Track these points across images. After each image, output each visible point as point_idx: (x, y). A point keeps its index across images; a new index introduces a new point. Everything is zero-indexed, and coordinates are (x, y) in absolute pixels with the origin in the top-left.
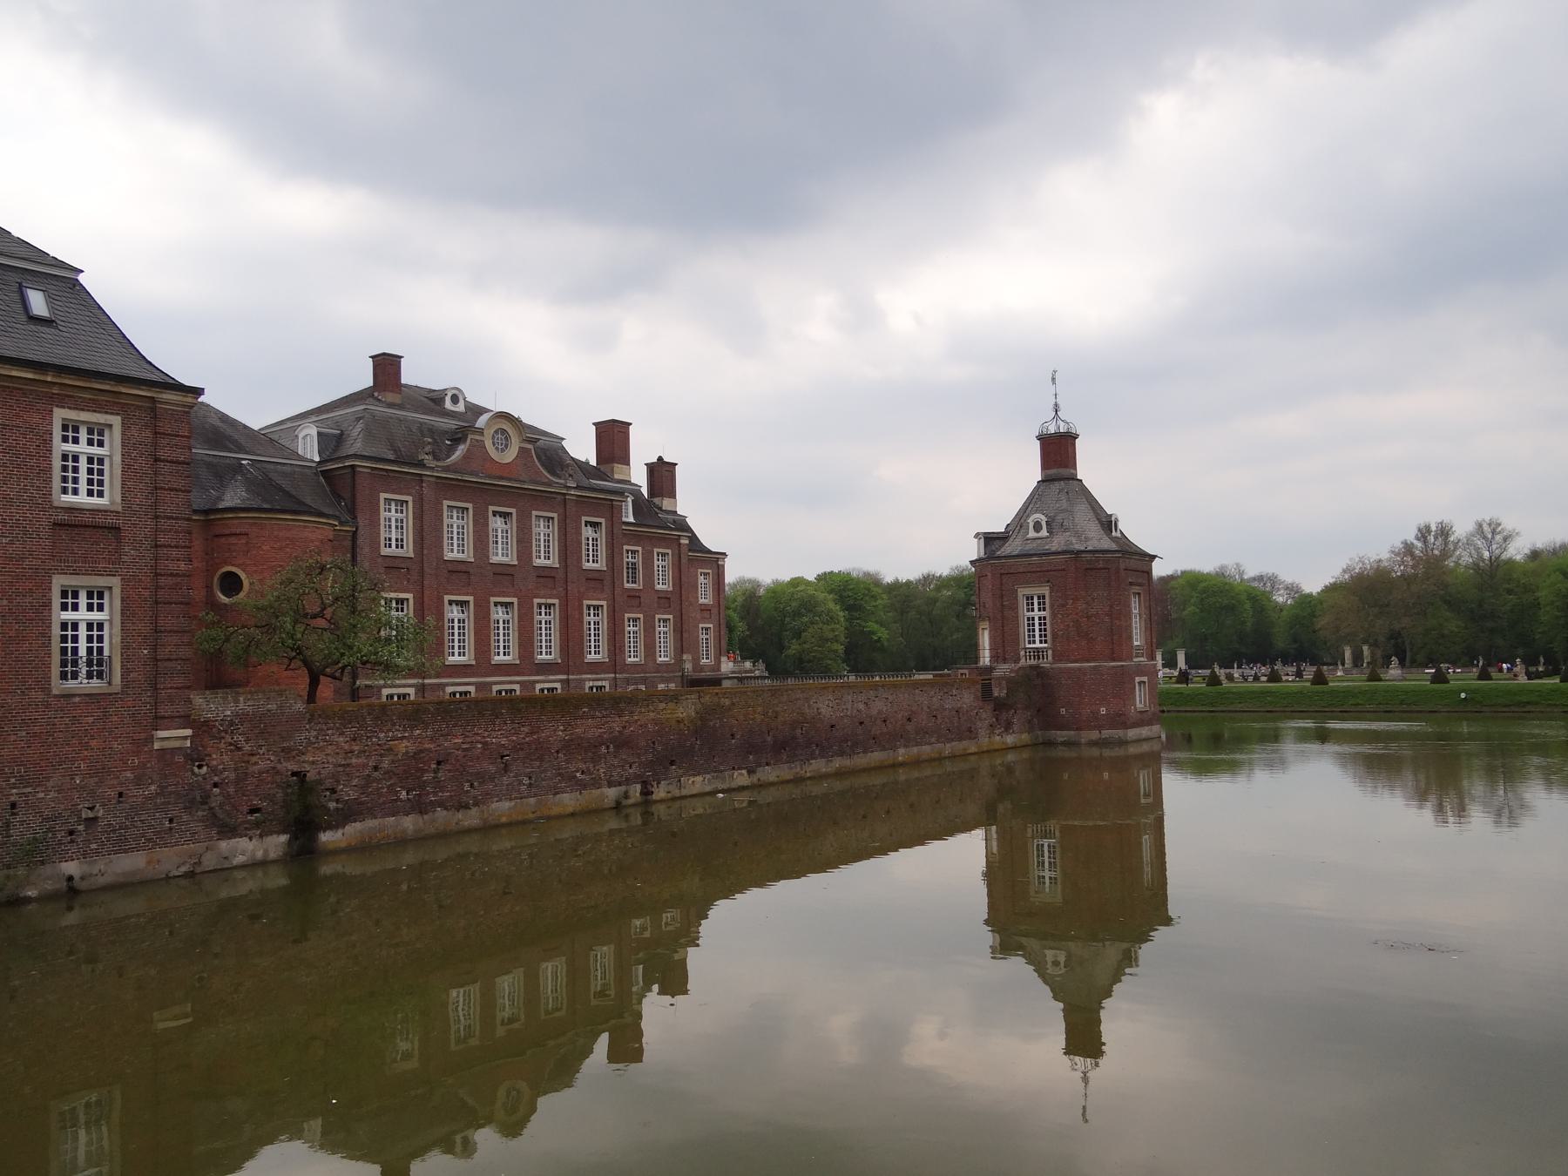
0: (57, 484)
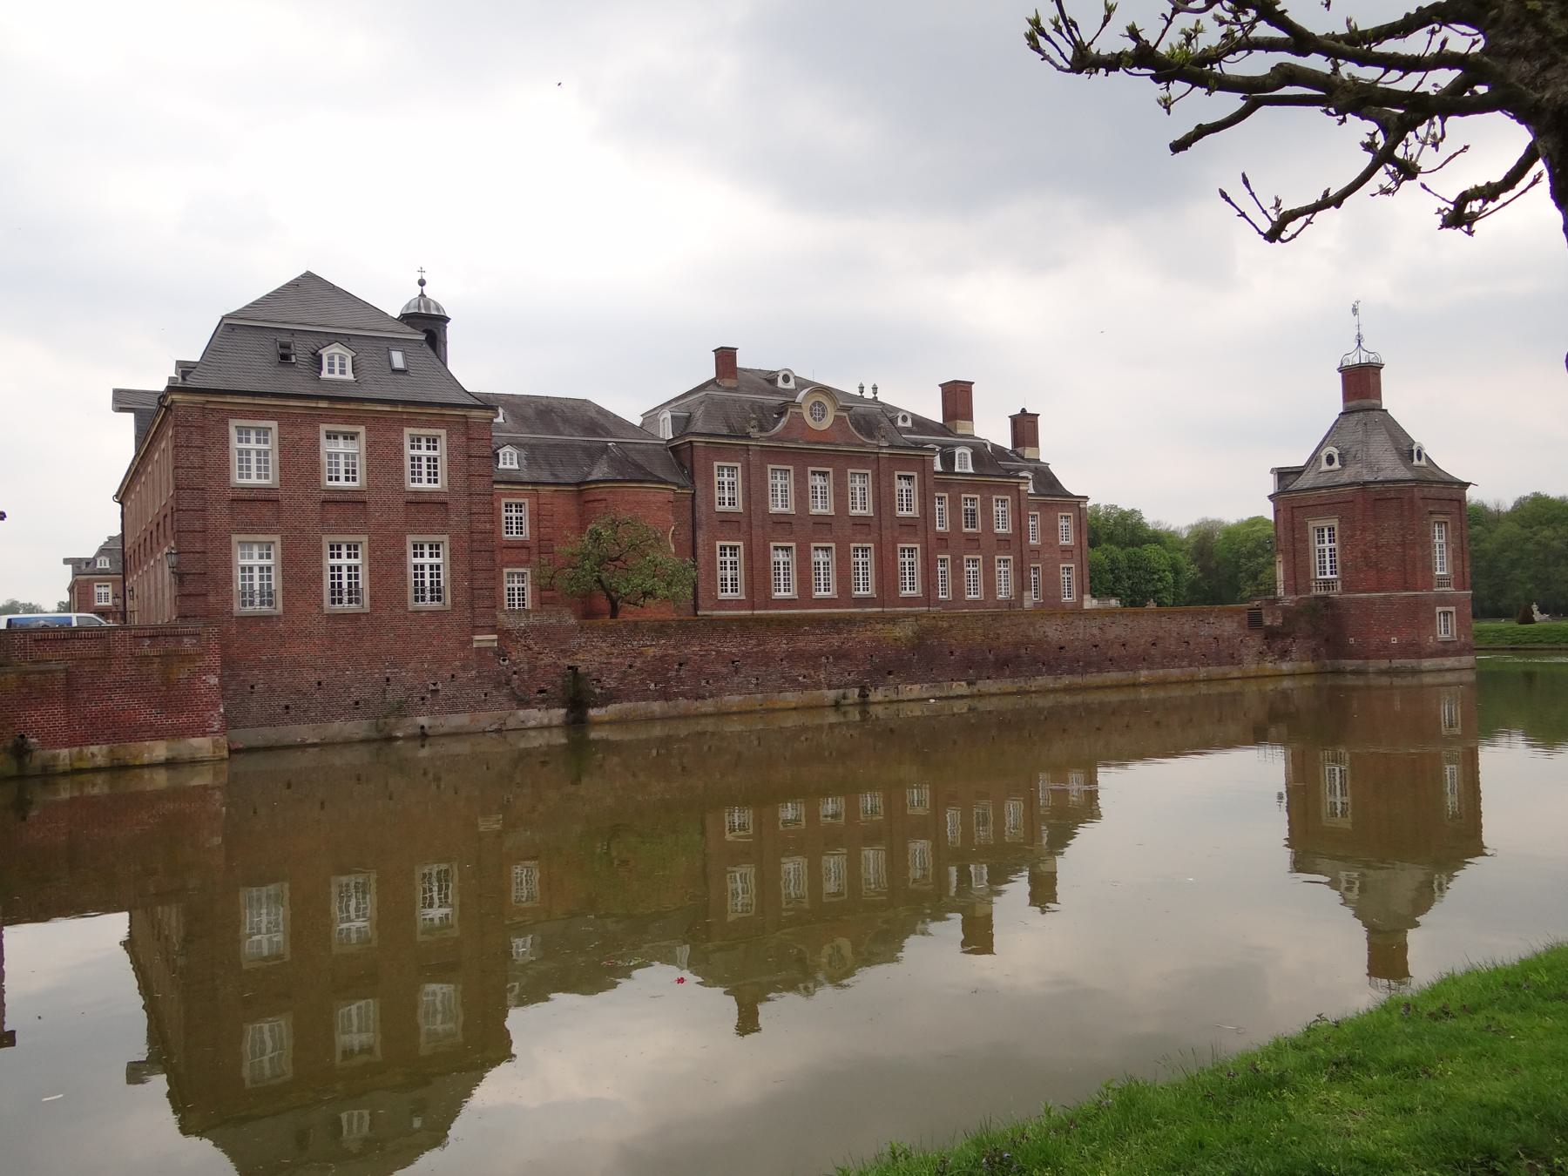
0: (408, 476)
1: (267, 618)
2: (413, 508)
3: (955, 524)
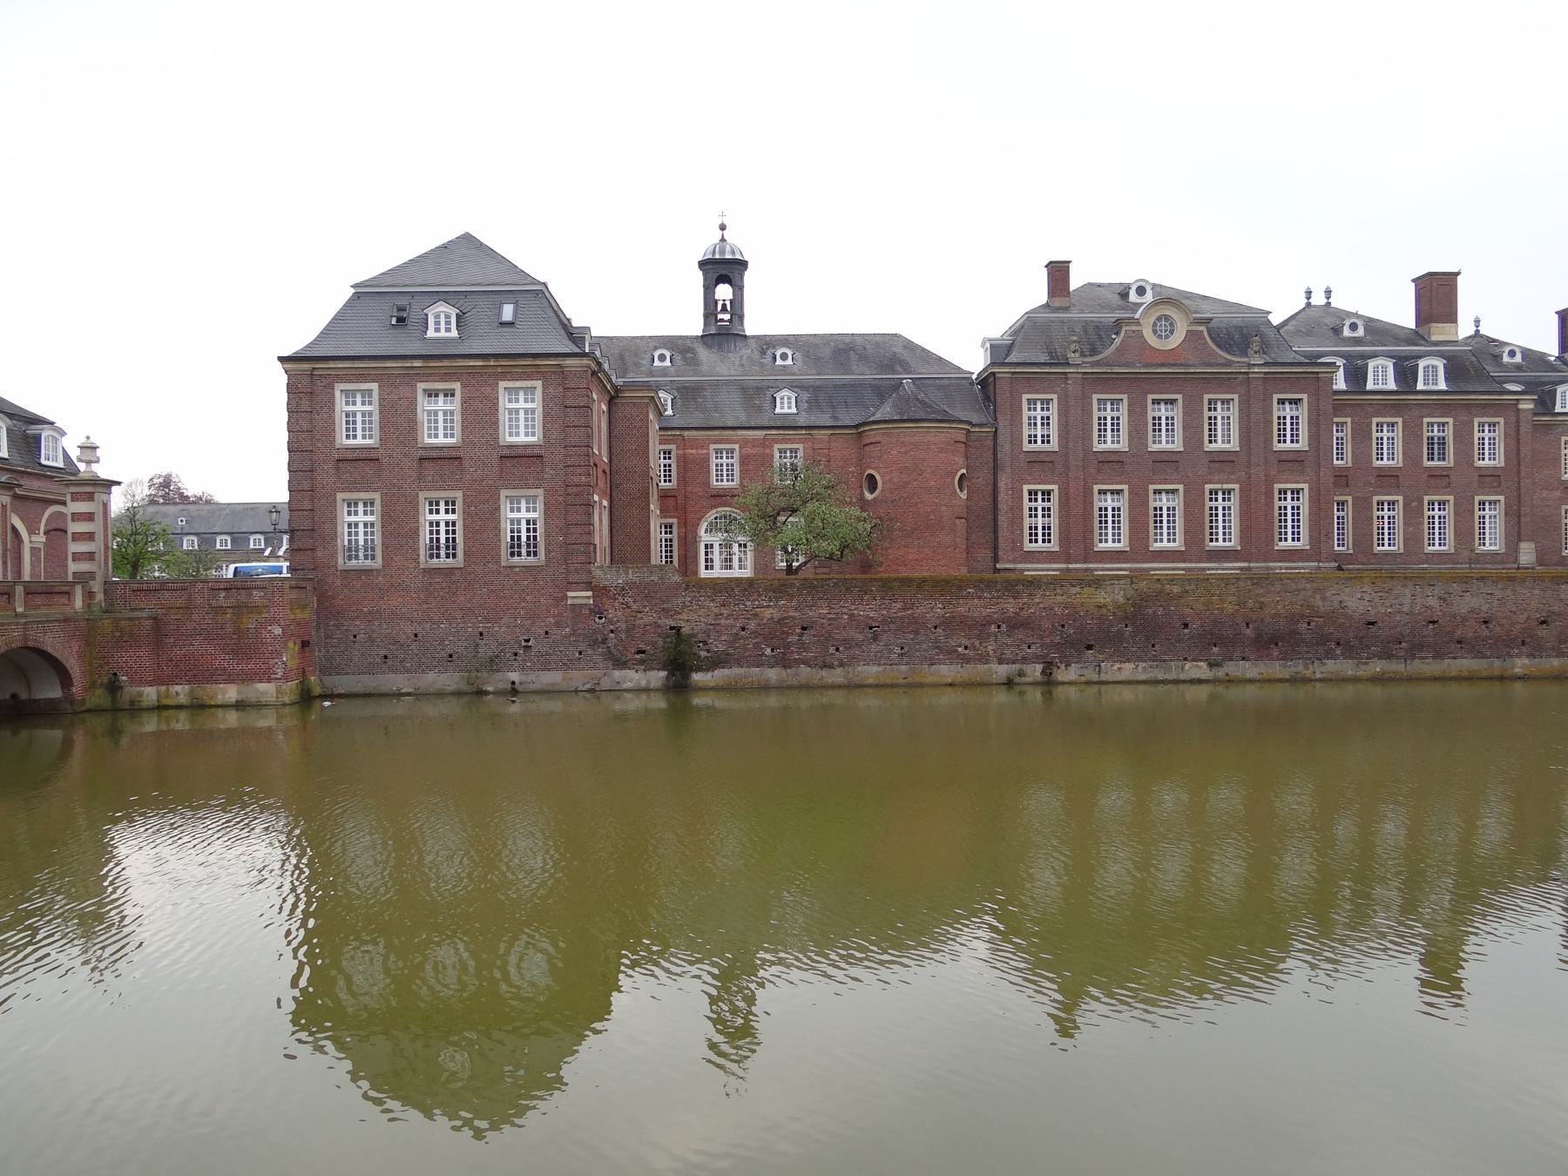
1: (368, 572)
2: (508, 463)
3: (1411, 457)
